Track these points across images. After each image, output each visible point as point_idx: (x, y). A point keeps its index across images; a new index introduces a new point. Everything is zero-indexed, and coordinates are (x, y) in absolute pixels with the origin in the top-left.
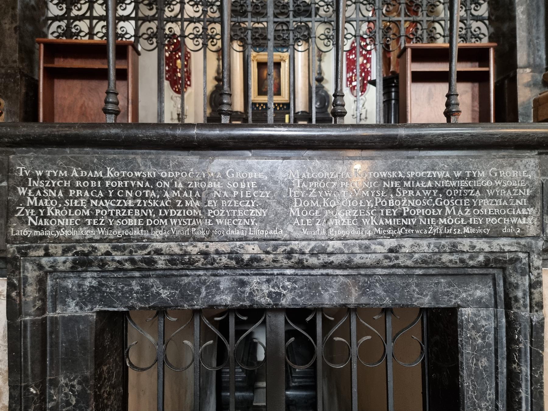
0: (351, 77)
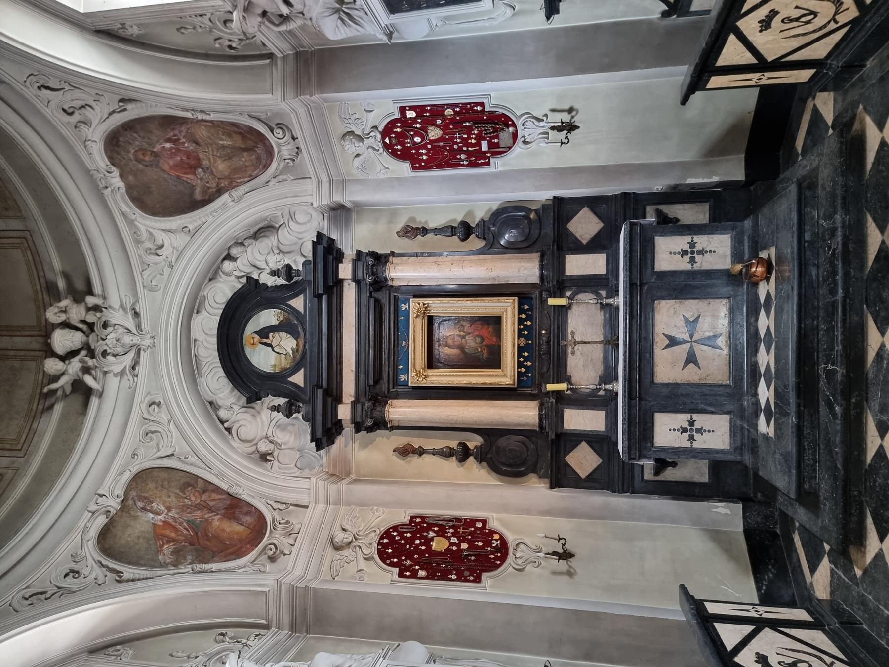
0: (469, 154)
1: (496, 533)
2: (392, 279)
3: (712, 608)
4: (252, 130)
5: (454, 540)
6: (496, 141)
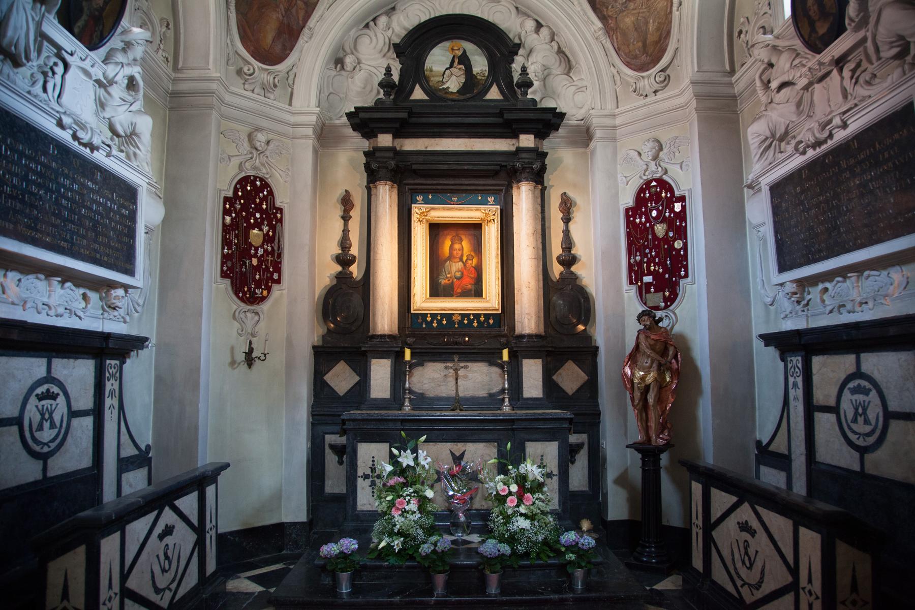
0: (640, 264)
1: (269, 293)
2: (519, 188)
3: (210, 490)
4: (663, 51)
5: (261, 252)
6: (652, 290)
